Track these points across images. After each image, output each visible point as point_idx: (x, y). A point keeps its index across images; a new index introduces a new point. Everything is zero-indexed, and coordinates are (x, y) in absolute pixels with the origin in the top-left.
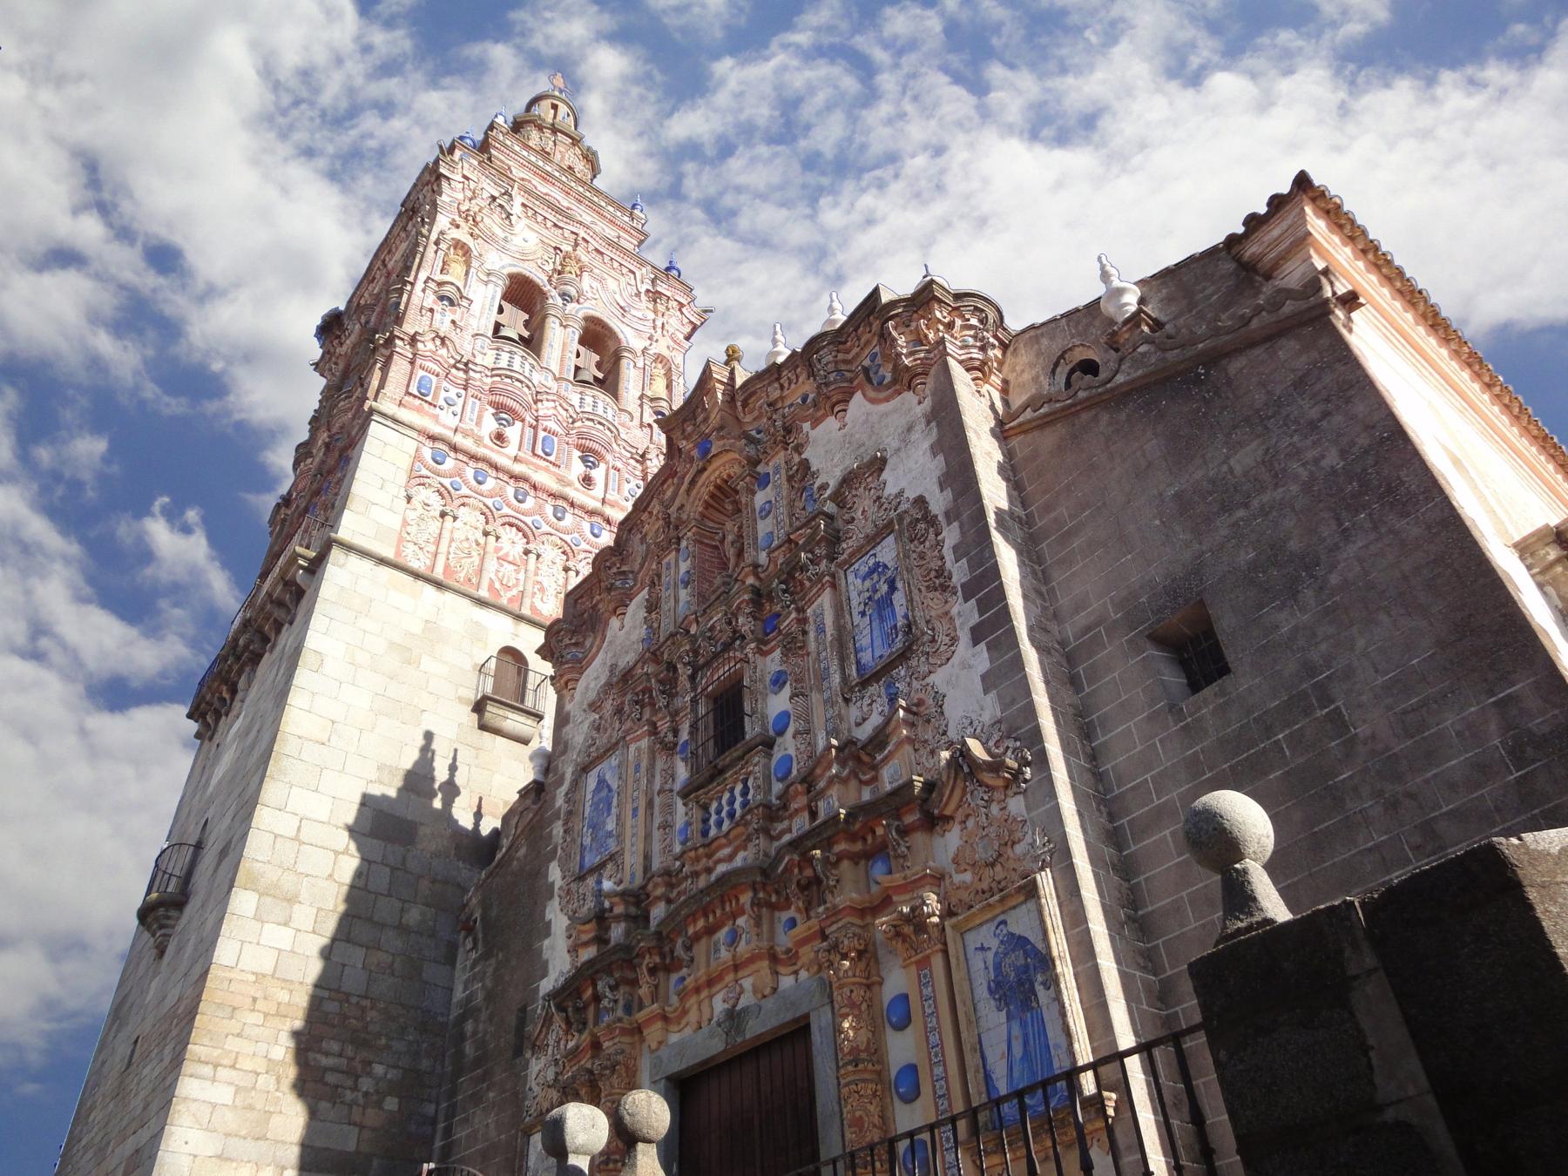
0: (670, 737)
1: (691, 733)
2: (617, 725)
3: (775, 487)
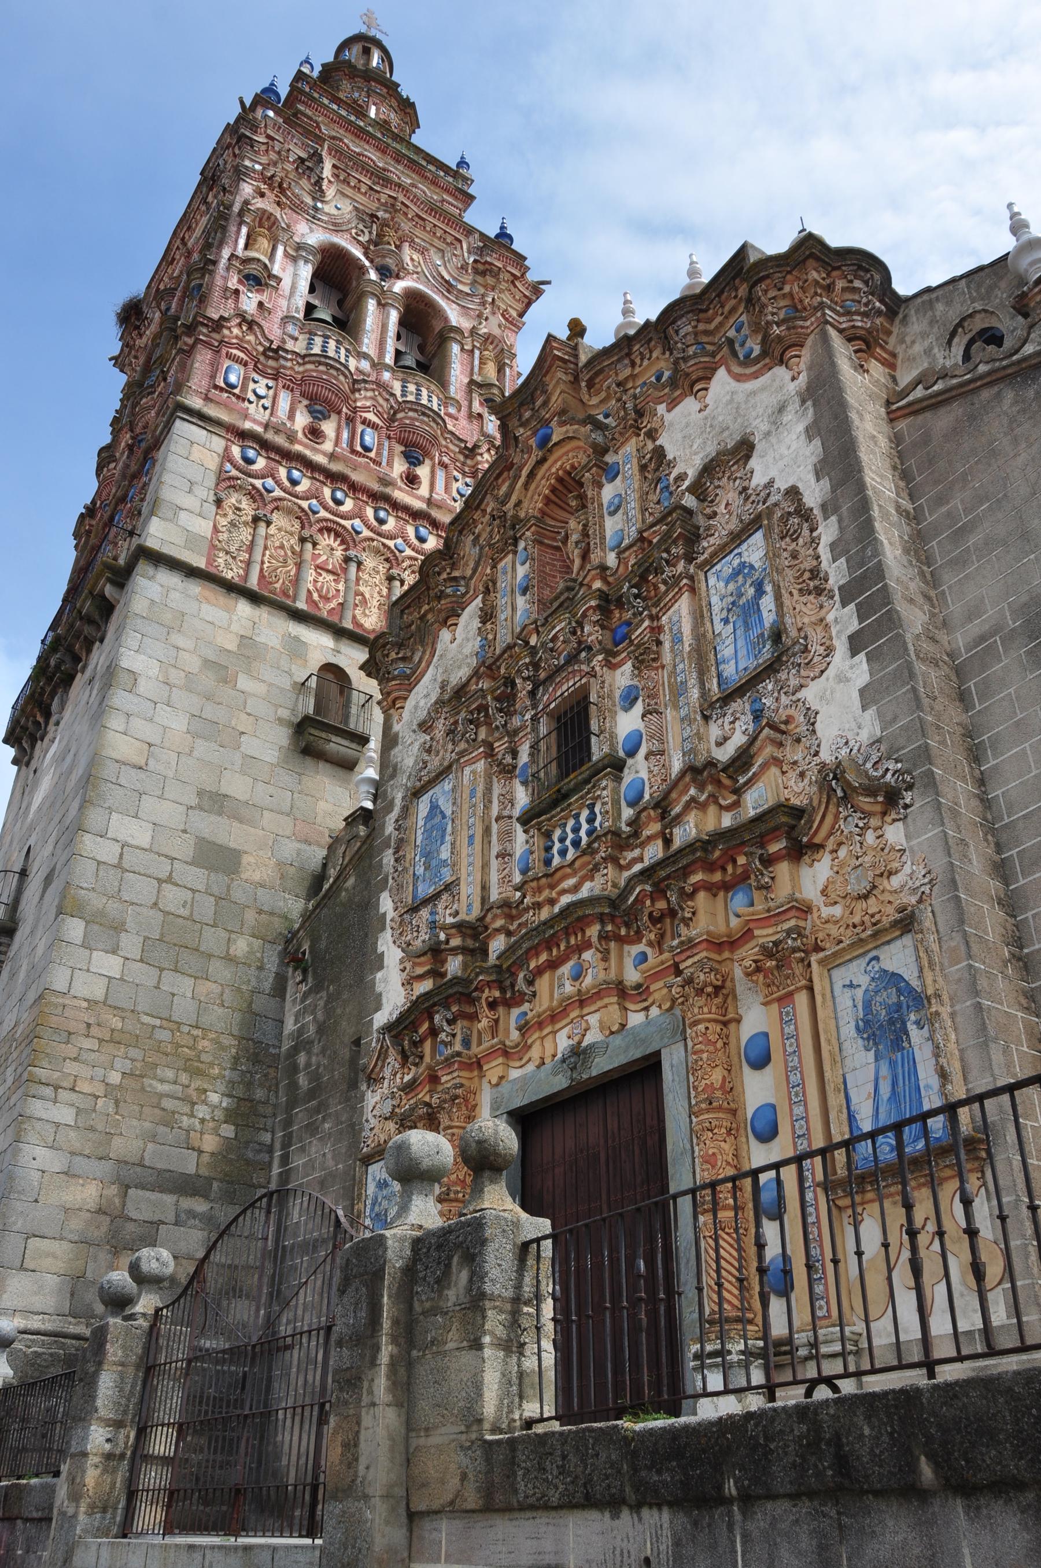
0: (508, 759)
1: (531, 755)
2: (450, 747)
3: (625, 479)
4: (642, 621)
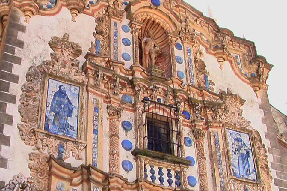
4: (202, 122)
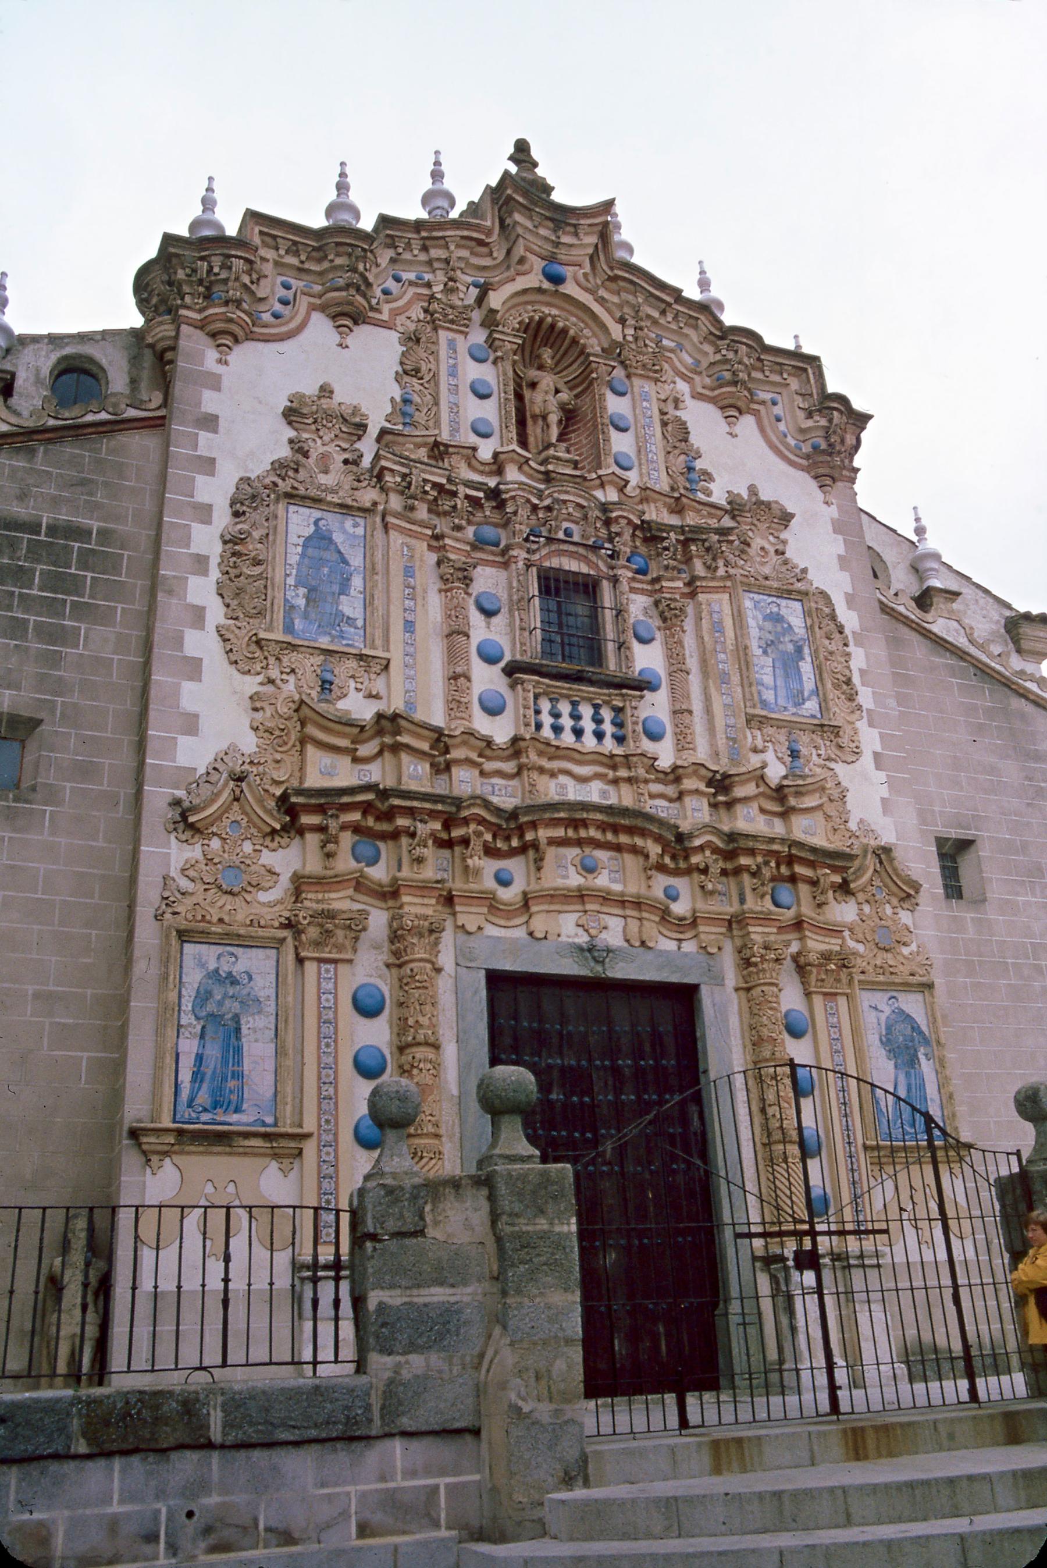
4: (679, 579)
